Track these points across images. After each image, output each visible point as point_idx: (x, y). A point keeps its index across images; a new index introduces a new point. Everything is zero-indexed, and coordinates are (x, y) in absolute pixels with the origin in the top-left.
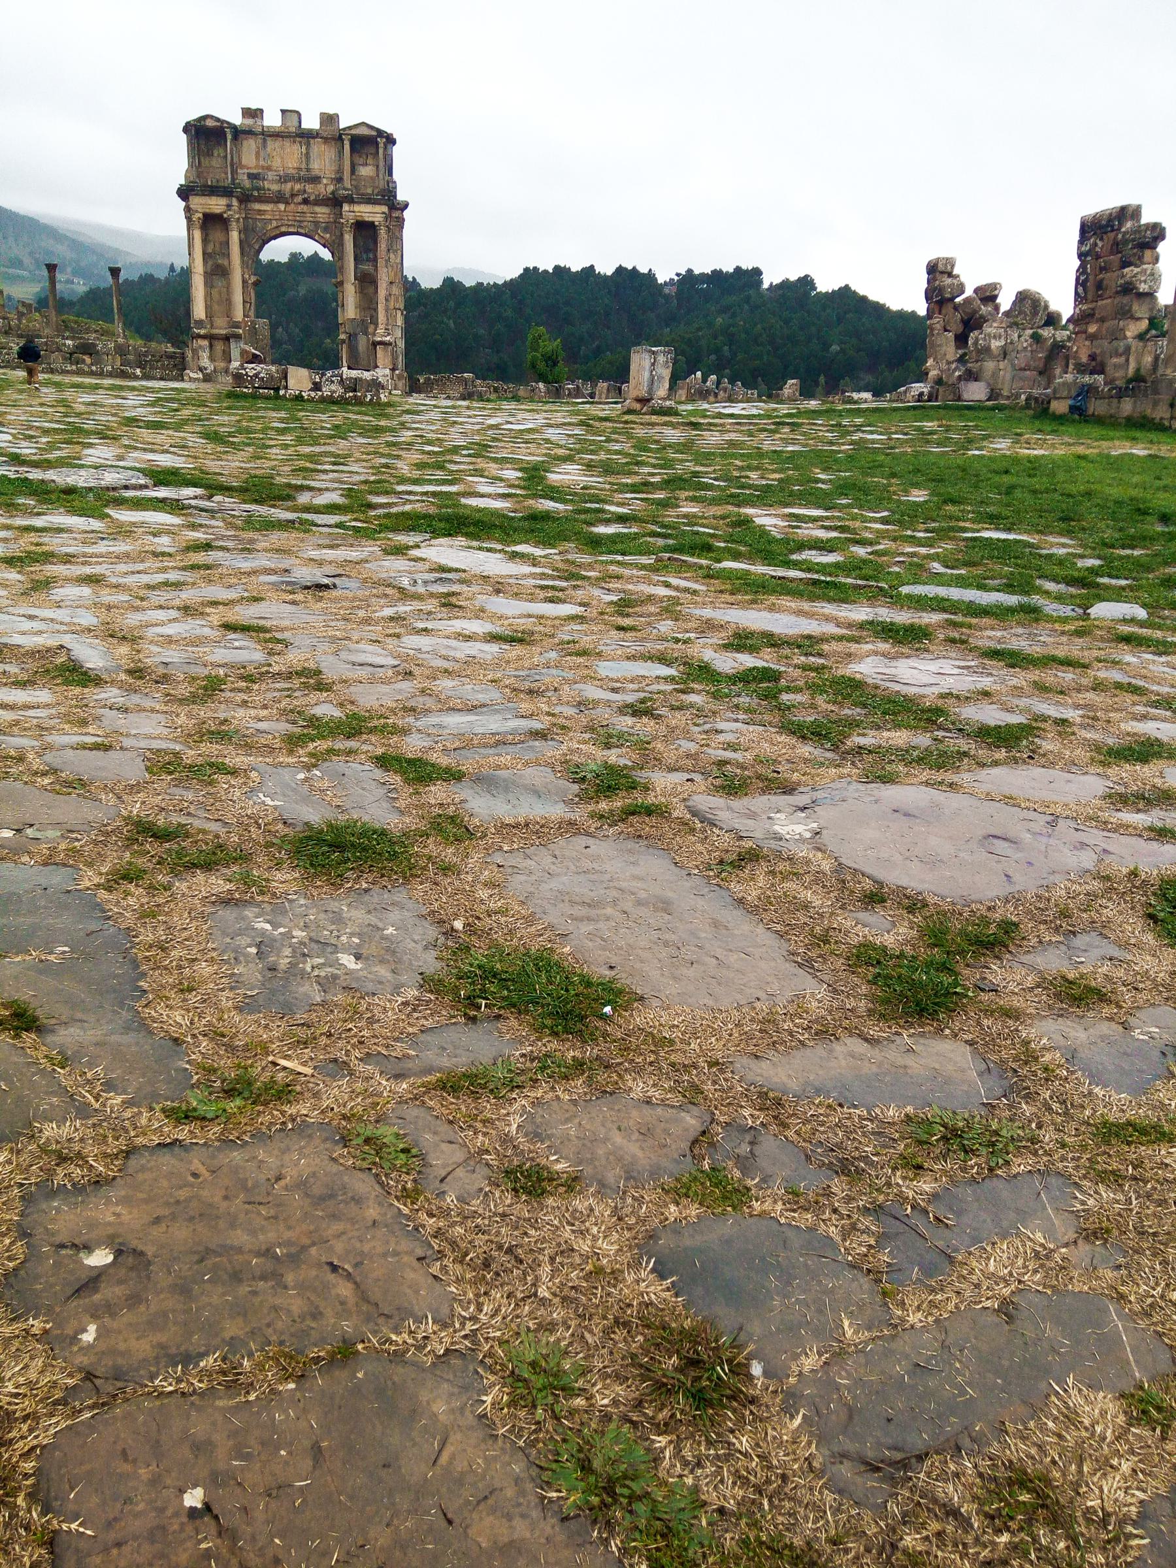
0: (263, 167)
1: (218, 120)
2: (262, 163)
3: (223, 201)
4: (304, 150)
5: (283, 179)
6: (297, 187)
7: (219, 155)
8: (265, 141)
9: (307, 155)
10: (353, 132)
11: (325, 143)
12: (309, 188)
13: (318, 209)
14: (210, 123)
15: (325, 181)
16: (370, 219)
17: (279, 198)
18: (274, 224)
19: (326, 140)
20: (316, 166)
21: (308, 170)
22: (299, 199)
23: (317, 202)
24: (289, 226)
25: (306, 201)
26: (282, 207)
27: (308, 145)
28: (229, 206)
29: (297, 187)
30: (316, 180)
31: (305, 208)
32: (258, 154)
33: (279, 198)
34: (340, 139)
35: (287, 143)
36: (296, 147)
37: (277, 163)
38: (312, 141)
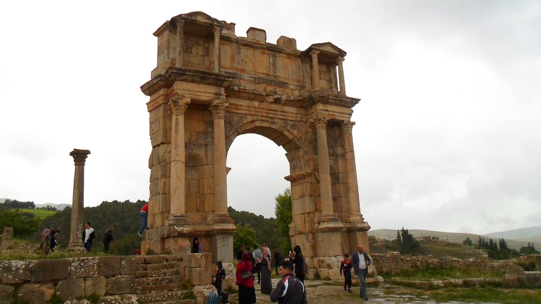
0: (237, 69)
1: (209, 17)
2: (236, 65)
3: (212, 89)
4: (271, 59)
5: (257, 80)
6: (269, 88)
7: (197, 54)
8: (239, 48)
9: (274, 65)
10: (321, 48)
11: (288, 58)
12: (279, 90)
13: (287, 109)
14: (200, 19)
15: (291, 87)
16: (340, 118)
17: (254, 96)
18: (250, 118)
19: (289, 55)
20: (282, 74)
21: (275, 77)
22: (271, 99)
23: (289, 103)
24: (263, 121)
25: (277, 101)
26: (256, 104)
27: (275, 57)
28: (218, 94)
29: (269, 88)
30: (283, 85)
31: (276, 107)
32: (233, 59)
33: (254, 96)
34: (306, 55)
35: (258, 53)
36: (266, 57)
37: (249, 67)
38: (278, 54)
